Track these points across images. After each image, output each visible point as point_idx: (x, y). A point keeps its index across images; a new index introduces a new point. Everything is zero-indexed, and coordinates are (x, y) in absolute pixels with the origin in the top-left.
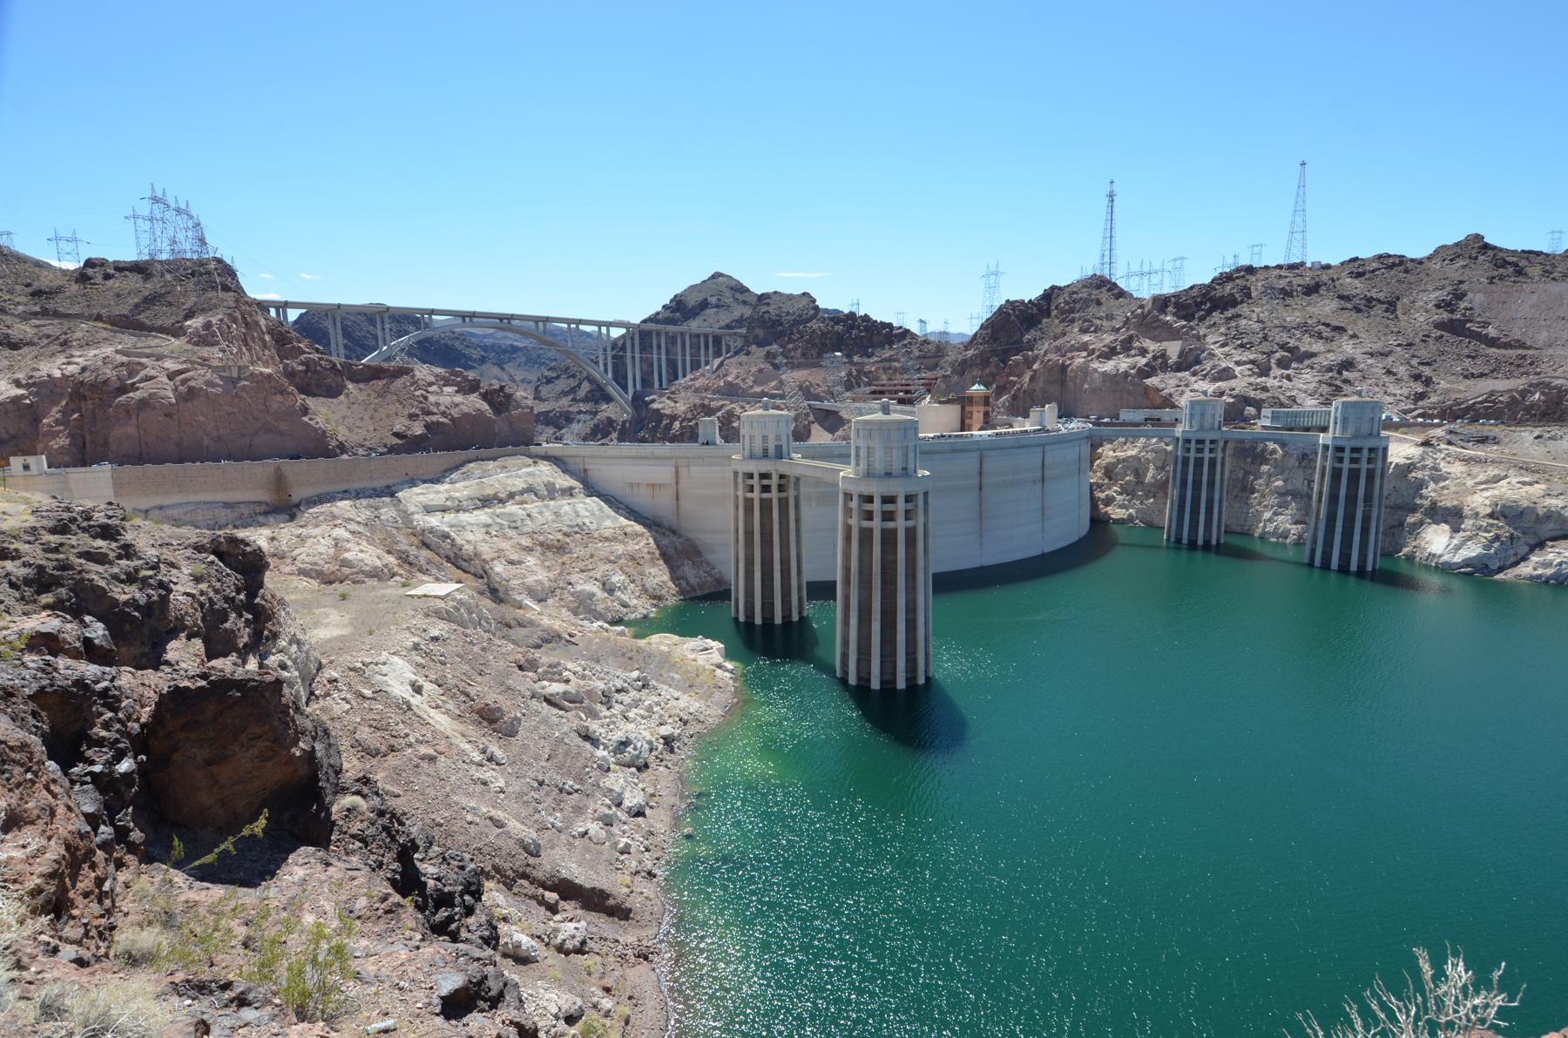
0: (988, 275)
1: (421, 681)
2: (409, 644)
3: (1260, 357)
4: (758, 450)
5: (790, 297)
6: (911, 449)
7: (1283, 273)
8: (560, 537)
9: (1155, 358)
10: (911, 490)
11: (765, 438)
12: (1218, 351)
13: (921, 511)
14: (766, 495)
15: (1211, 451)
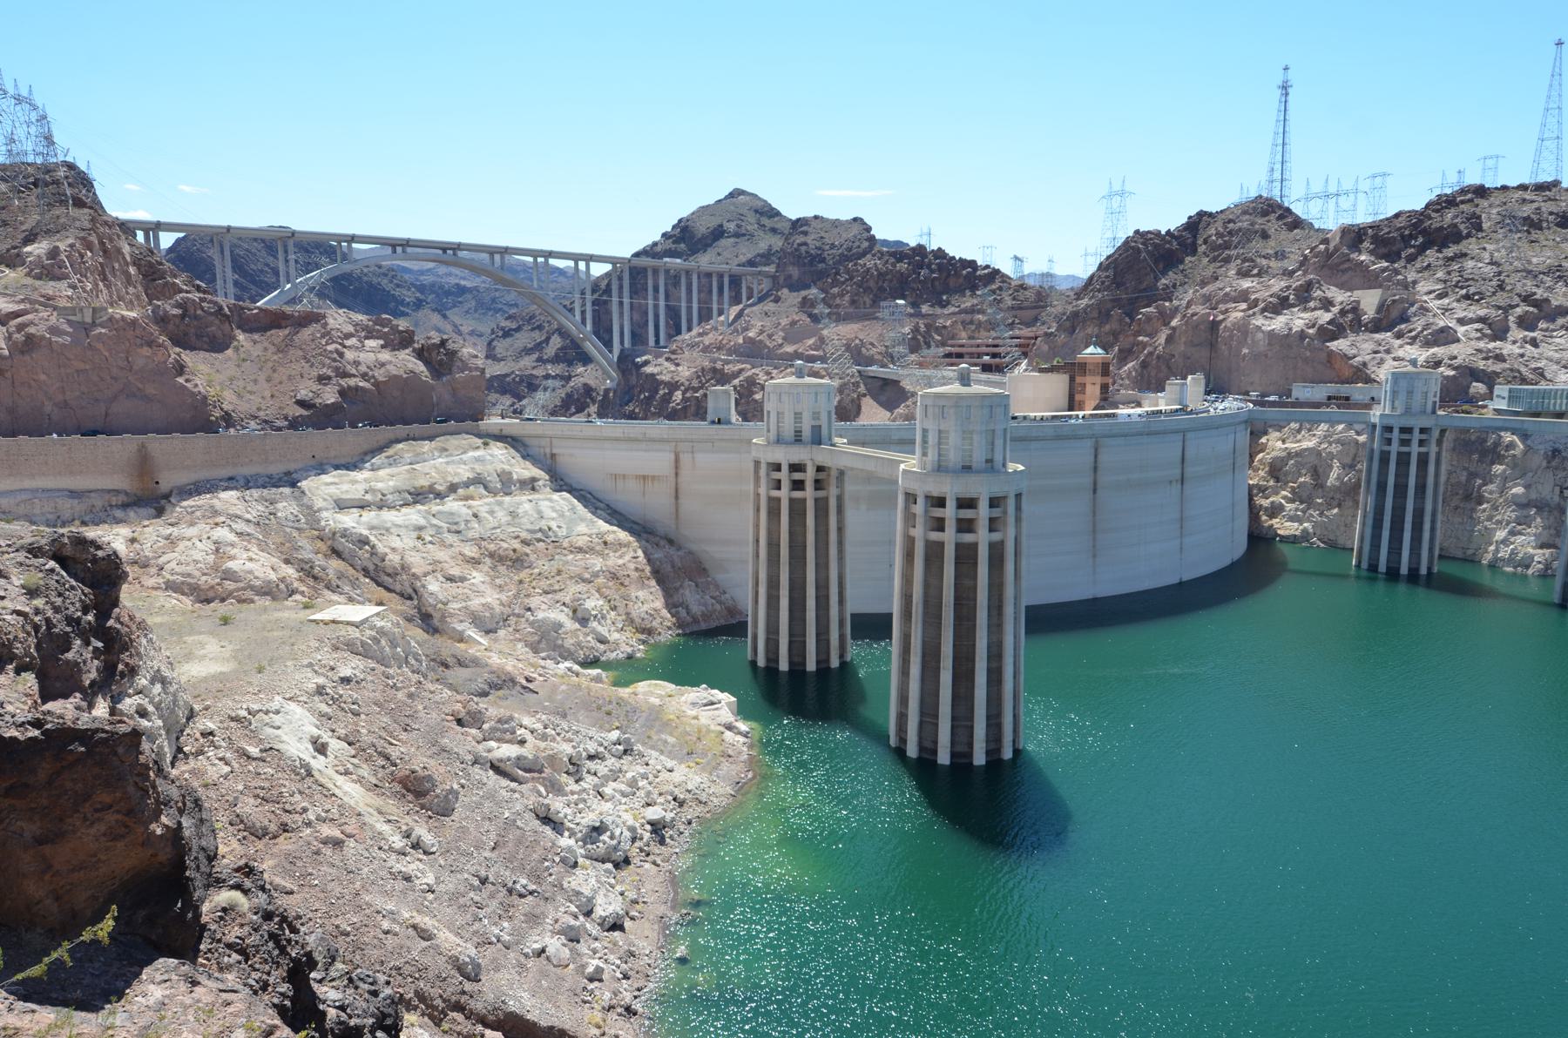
0: (1110, 196)
1: (326, 737)
2: (311, 686)
3: (1493, 313)
4: (788, 430)
5: (836, 224)
6: (999, 433)
7: (1528, 196)
8: (516, 545)
9: (1343, 312)
10: (998, 490)
11: (798, 416)
12: (1434, 304)
13: (1011, 519)
14: (798, 494)
15: (1421, 443)
